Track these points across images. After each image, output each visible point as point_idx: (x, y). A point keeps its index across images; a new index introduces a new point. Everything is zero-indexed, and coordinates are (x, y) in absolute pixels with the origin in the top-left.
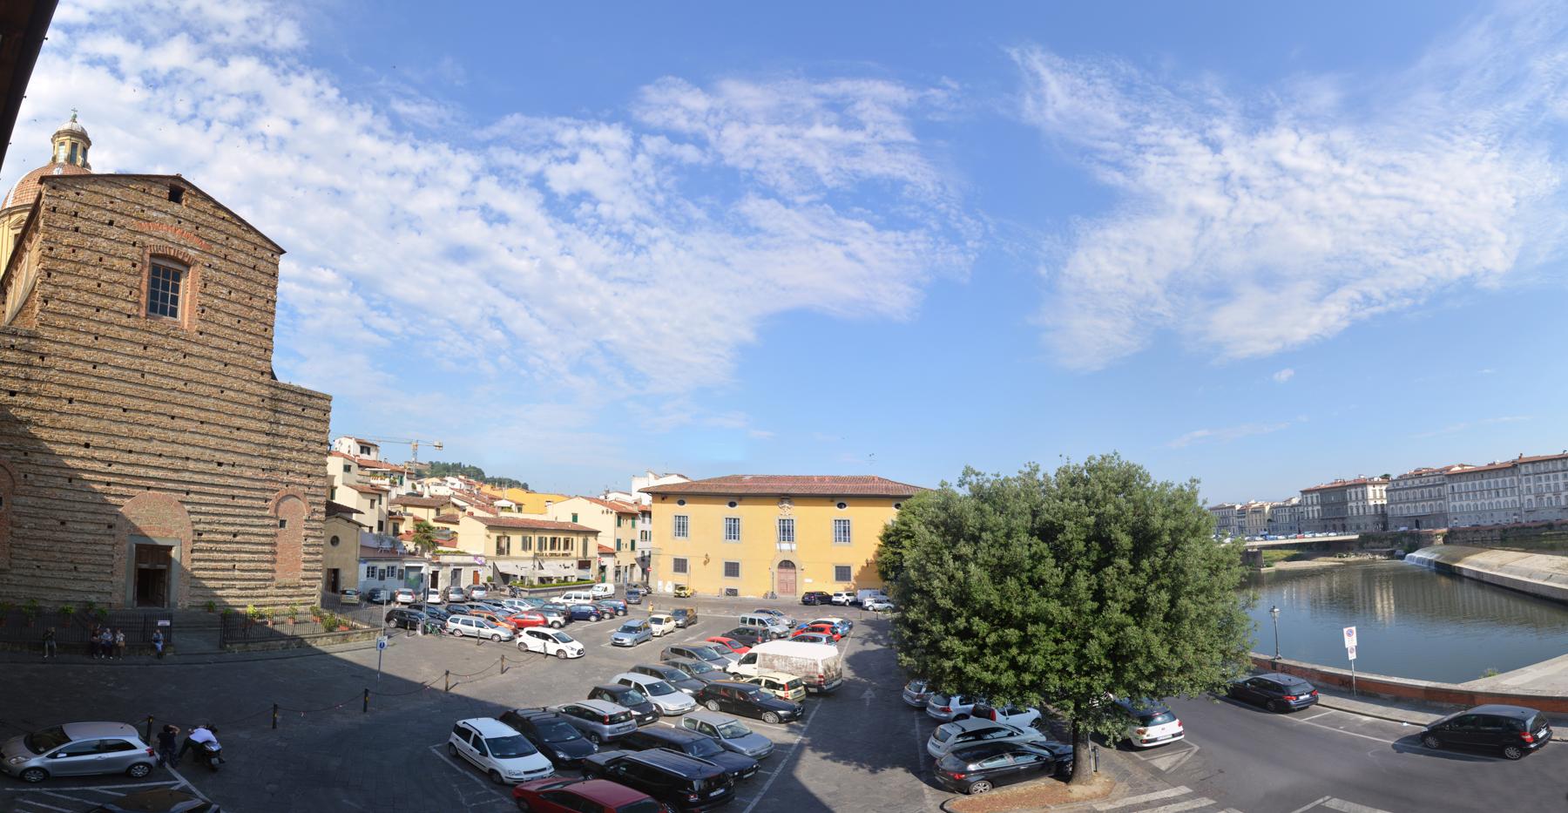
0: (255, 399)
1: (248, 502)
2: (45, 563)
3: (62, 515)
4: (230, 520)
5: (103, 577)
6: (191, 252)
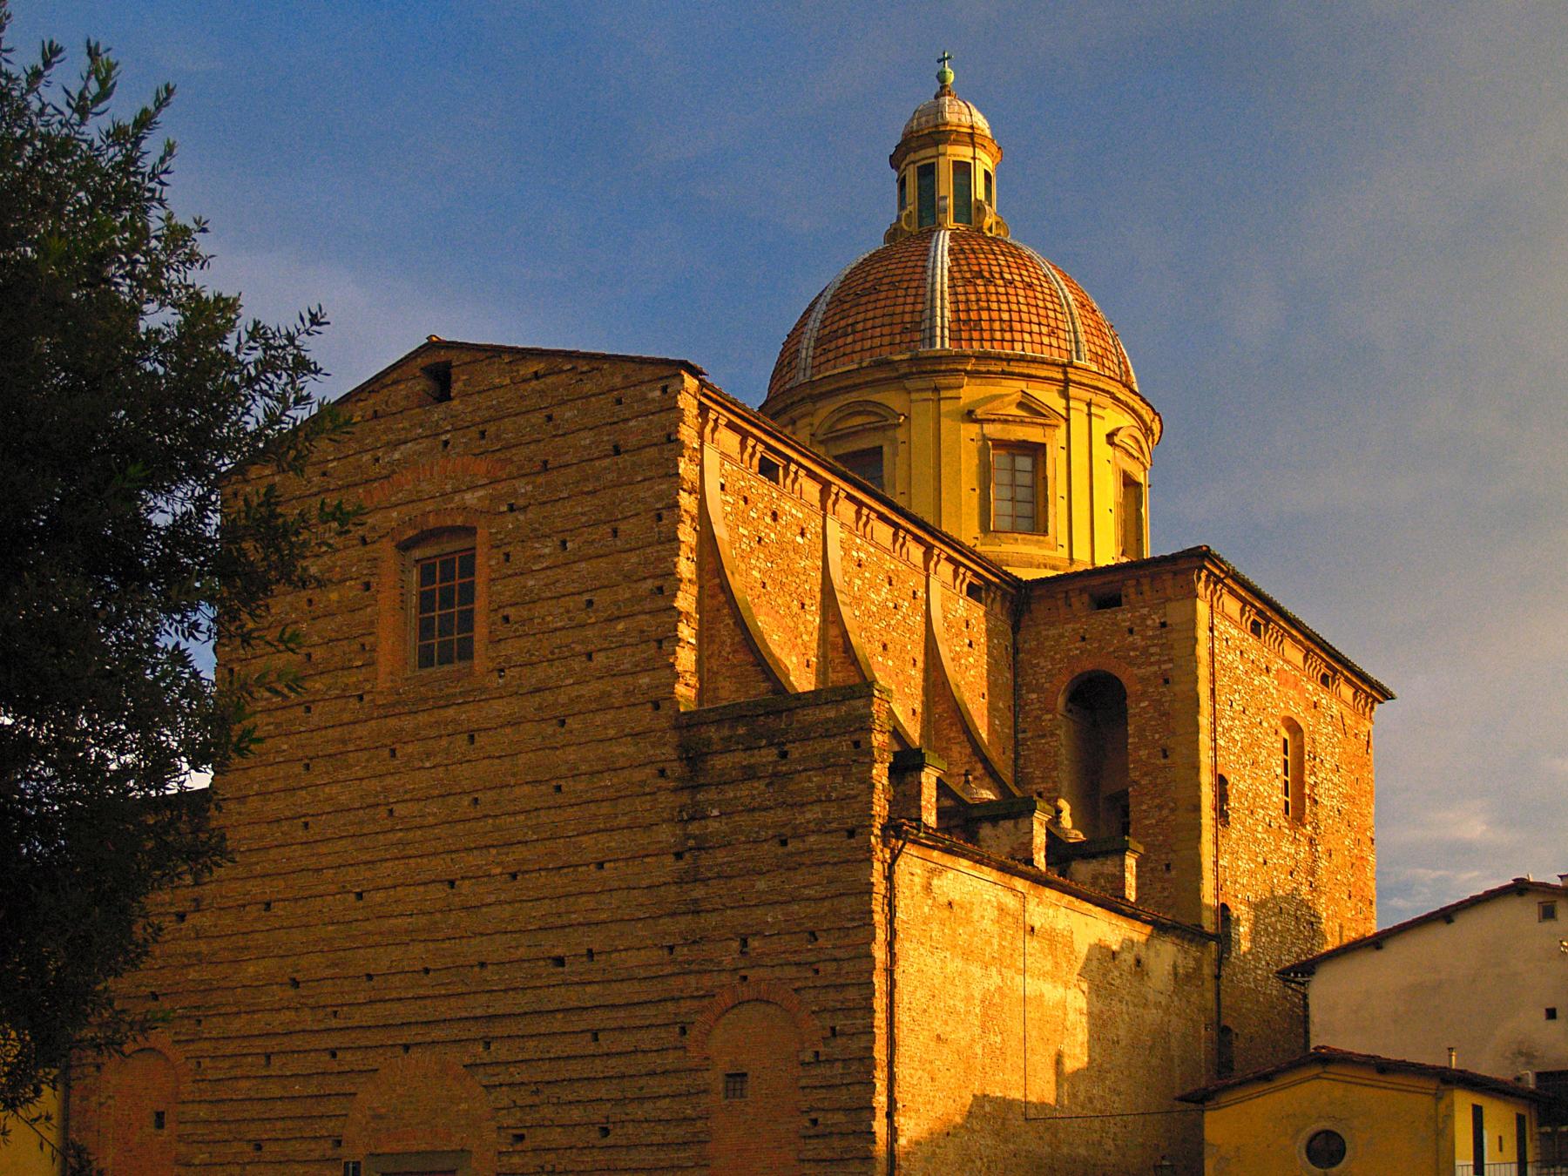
0: (638, 775)
1: (626, 1041)
4: (584, 1092)
6: (471, 498)
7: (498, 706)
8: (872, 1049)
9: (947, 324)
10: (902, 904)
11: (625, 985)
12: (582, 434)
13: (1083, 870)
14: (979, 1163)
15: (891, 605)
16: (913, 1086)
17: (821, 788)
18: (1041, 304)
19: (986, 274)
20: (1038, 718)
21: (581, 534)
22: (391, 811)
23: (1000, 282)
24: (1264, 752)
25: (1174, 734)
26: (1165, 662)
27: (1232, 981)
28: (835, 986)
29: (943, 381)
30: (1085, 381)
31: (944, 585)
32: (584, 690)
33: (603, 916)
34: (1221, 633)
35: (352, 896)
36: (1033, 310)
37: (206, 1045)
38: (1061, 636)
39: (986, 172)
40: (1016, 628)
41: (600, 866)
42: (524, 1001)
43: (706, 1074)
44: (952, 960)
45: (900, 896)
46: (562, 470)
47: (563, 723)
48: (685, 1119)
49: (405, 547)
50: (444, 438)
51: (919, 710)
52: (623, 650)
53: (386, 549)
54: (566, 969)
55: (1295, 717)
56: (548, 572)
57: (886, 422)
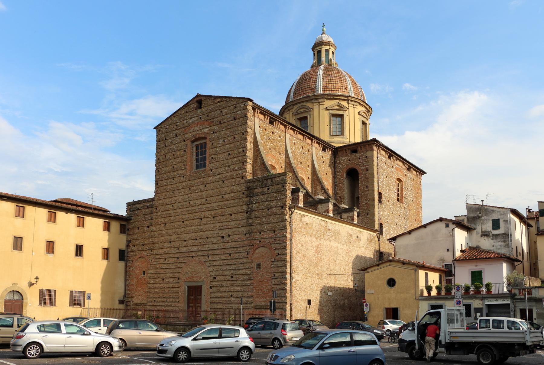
0: (239, 194)
1: (237, 255)
2: (157, 299)
3: (162, 276)
4: (228, 267)
5: (176, 304)
6: (206, 130)
7: (210, 178)
8: (286, 258)
9: (321, 87)
10: (294, 224)
11: (236, 243)
12: (228, 115)
13: (345, 216)
14: (314, 285)
15: (303, 153)
16: (297, 267)
17: (276, 197)
18: (343, 82)
19: (330, 75)
20: (340, 179)
21: (228, 138)
22: (189, 202)
23: (334, 77)
24: (392, 187)
25: (369, 182)
26: (367, 166)
27: (383, 241)
28: (279, 243)
29: (320, 100)
30: (353, 100)
31: (316, 148)
32: (228, 174)
33: (231, 227)
34: (380, 159)
35: (182, 222)
36: (341, 83)
37: (153, 256)
38: (345, 160)
39: (332, 52)
40: (335, 158)
41: (231, 215)
42: (216, 246)
43: (252, 264)
44: (307, 237)
45: (293, 222)
46: (224, 124)
47: (224, 182)
48: (248, 274)
49: (193, 142)
50: (200, 117)
51: (310, 177)
52: (236, 165)
53: (189, 143)
54: (224, 239)
55: (400, 178)
56: (221, 147)
57: (309, 110)
